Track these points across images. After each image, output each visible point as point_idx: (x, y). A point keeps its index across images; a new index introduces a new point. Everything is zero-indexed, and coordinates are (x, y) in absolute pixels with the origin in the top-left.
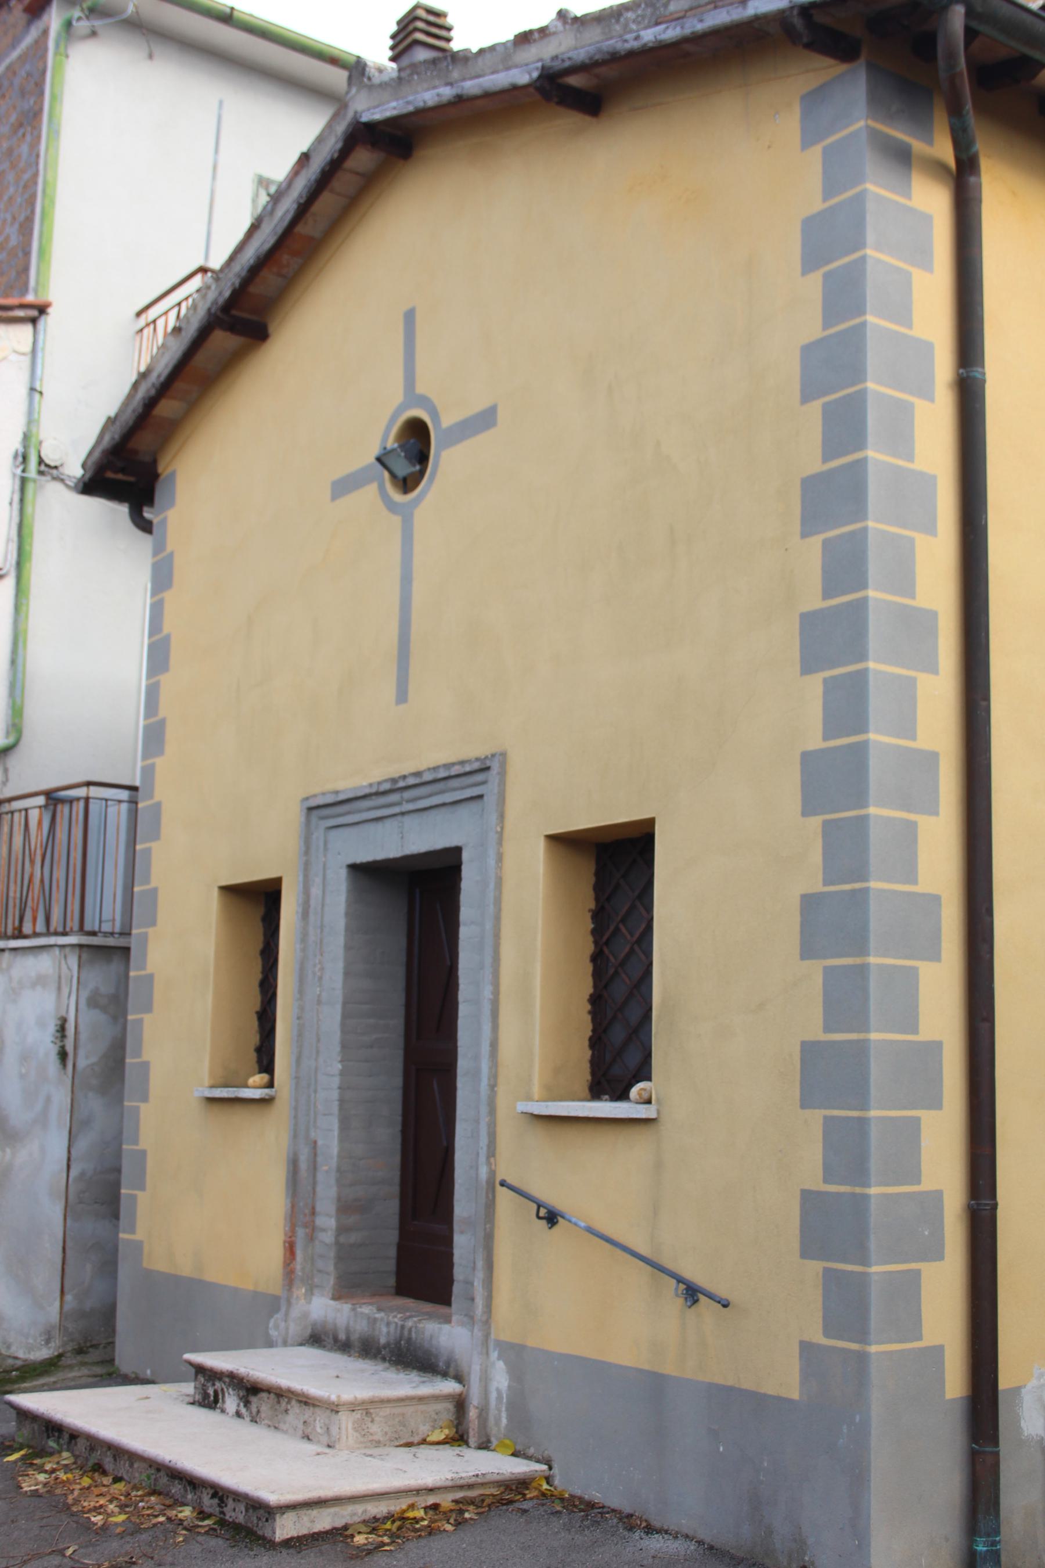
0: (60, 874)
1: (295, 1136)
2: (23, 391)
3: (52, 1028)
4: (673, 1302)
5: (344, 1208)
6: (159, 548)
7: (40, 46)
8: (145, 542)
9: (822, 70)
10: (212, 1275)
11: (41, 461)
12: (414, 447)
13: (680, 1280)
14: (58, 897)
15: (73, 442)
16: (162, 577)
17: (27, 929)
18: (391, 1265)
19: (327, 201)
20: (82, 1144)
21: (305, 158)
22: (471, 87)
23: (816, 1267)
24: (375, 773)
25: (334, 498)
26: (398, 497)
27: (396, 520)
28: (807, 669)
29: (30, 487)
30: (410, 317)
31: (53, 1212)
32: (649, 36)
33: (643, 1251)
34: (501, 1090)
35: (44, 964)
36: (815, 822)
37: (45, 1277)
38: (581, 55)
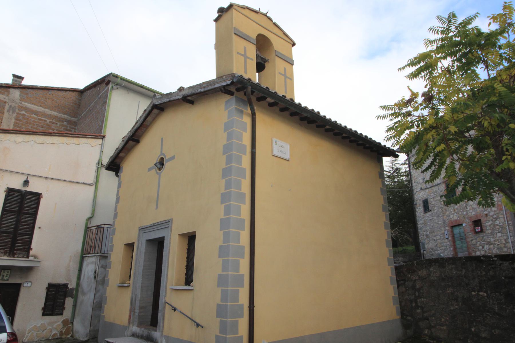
0: (98, 242)
1: (132, 293)
2: (99, 151)
3: (93, 272)
4: (194, 327)
5: (140, 308)
6: (119, 180)
7: (107, 90)
8: (117, 179)
9: (228, 97)
10: (117, 322)
11: (102, 164)
12: (161, 163)
13: (195, 322)
14: (97, 246)
15: (106, 161)
16: (119, 186)
17: (91, 252)
18: (150, 320)
19: (149, 118)
20: (97, 295)
21: (145, 110)
22: (172, 99)
23: (219, 319)
24: (151, 222)
25: (148, 171)
26: (158, 171)
27: (158, 176)
28: (222, 204)
29: (99, 169)
30: (162, 139)
31: (90, 309)
32: (199, 90)
33: (190, 316)
34: (168, 284)
35: (93, 259)
36: (222, 232)
37: (87, 323)
38: (189, 94)
